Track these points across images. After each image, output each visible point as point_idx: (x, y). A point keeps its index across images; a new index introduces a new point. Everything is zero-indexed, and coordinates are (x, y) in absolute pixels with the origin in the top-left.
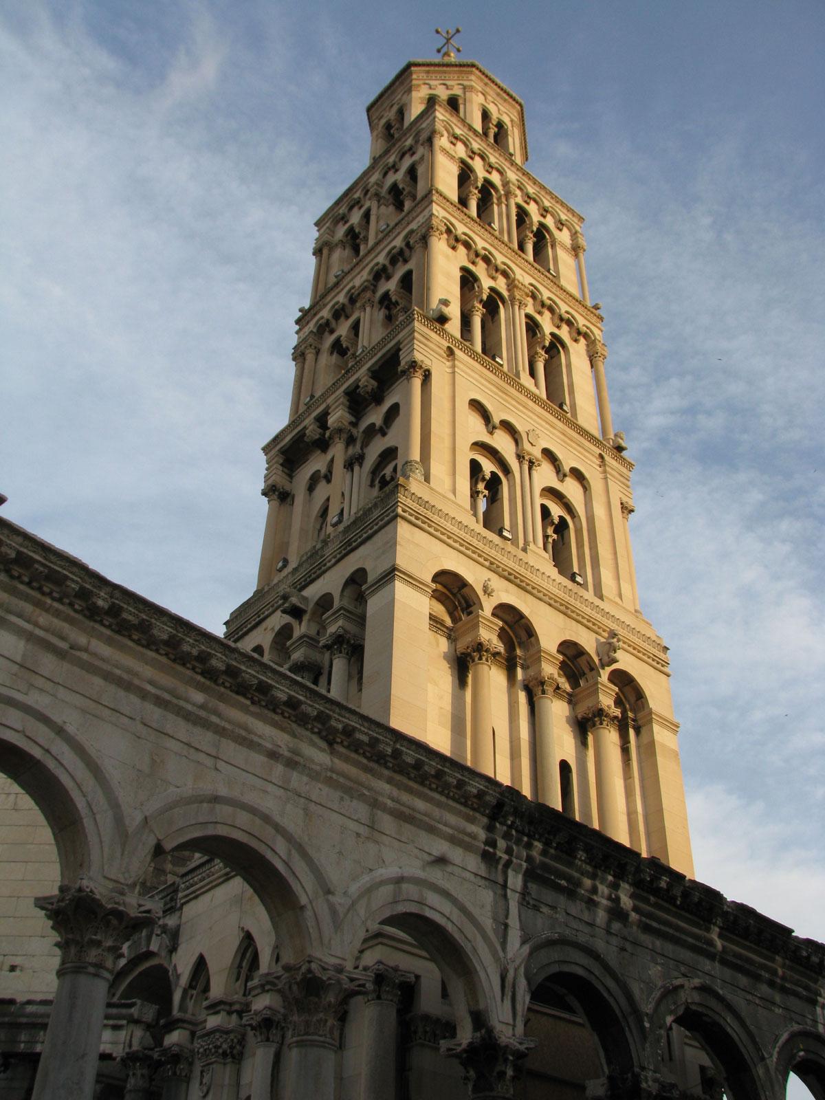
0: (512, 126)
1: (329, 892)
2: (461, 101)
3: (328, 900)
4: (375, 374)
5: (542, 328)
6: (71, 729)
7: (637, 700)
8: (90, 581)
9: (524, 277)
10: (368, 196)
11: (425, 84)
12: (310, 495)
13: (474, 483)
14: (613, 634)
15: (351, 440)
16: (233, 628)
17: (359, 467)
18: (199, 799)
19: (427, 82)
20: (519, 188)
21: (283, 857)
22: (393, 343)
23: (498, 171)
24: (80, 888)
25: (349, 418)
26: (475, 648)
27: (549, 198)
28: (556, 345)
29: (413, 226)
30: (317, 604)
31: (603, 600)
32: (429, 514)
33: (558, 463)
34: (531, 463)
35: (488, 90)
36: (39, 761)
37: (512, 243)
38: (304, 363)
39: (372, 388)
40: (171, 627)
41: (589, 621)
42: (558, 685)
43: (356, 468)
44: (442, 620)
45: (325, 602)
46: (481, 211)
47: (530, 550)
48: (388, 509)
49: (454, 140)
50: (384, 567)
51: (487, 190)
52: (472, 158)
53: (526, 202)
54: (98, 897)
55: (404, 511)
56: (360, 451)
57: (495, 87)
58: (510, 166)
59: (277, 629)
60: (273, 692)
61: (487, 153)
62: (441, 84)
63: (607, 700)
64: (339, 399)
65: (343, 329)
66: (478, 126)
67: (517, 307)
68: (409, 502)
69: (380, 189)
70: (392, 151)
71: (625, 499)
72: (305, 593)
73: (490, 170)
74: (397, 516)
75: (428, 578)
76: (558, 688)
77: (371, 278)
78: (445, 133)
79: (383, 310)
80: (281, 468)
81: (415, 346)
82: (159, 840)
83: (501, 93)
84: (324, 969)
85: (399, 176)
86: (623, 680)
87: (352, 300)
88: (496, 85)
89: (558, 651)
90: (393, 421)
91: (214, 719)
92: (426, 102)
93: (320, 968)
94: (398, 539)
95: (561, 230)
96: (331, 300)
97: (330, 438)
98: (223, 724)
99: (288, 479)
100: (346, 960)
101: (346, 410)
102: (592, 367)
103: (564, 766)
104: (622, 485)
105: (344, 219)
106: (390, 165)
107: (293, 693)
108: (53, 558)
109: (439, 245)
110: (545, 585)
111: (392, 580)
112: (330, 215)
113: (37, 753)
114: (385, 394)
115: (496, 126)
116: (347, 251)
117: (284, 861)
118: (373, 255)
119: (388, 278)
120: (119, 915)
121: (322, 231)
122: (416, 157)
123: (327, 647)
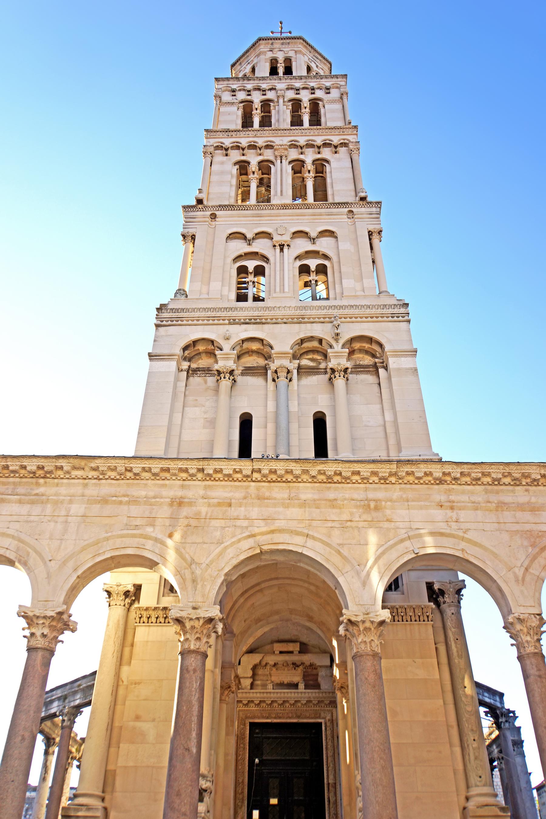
33: (309, 234)
34: (282, 247)
44: (208, 368)
49: (233, 94)
53: (297, 94)
57: (279, 41)
58: (279, 81)
71: (371, 228)
73: (264, 93)
95: (329, 93)
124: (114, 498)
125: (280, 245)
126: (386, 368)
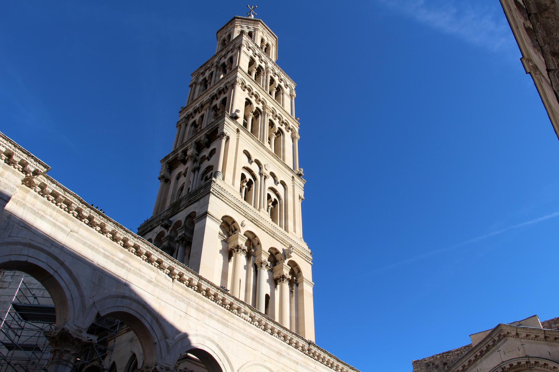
0: (272, 46)
1: (166, 337)
2: (253, 34)
3: (166, 341)
4: (207, 136)
5: (275, 126)
6: (67, 264)
7: (298, 273)
8: (82, 205)
9: (270, 104)
10: (213, 66)
11: (240, 26)
12: (177, 181)
13: (242, 182)
14: (291, 246)
15: (195, 161)
17: (197, 172)
18: (117, 297)
19: (241, 25)
20: (272, 70)
21: (150, 323)
22: (216, 124)
23: (265, 62)
24: (63, 328)
25: (196, 152)
26: (236, 247)
27: (283, 75)
28: (280, 132)
29: (229, 80)
30: (175, 224)
31: (288, 233)
32: (223, 193)
35: (264, 31)
36: (52, 275)
37: (267, 91)
38: (180, 129)
39: (206, 142)
40: (114, 227)
41: (282, 241)
42: (267, 264)
43: (196, 172)
45: (178, 223)
46: (257, 77)
47: (262, 211)
48: (206, 190)
50: (202, 212)
51: (260, 69)
52: (255, 57)
53: (274, 76)
54: (70, 332)
55: (213, 191)
56: (199, 166)
59: (158, 232)
60: (152, 256)
61: (262, 55)
62: (246, 27)
63: (286, 271)
64: (192, 145)
65: (197, 117)
66: (259, 44)
67: (266, 116)
68: (215, 187)
69: (218, 64)
70: (224, 50)
72: (170, 219)
73: (262, 62)
74: (210, 192)
75: (220, 218)
76: (267, 265)
77: (210, 98)
78: (246, 46)
79: (214, 111)
80: (167, 169)
81: (224, 127)
82: (99, 311)
83: (269, 33)
84: (162, 368)
85: (225, 60)
86: (293, 264)
87: (202, 106)
88: (268, 29)
89: (269, 251)
90: (213, 155)
91: (127, 265)
92: (240, 32)
93: (160, 368)
94: (210, 201)
95: (287, 88)
96: (194, 105)
97: (187, 159)
98: (130, 267)
99: (169, 173)
100: (170, 365)
101: (195, 149)
102: (293, 142)
103: (267, 297)
104: (300, 189)
105: (203, 74)
106: (223, 55)
107: (160, 257)
108: (68, 194)
109: (238, 88)
110: (266, 224)
111: (206, 217)
113: (51, 272)
115: (266, 45)
116: (202, 86)
117: (149, 324)
118: (212, 90)
119: (217, 99)
120: (79, 341)
122: (233, 54)
123: (177, 241)
124: (257, 339)
125: (265, 176)
126: (297, 285)
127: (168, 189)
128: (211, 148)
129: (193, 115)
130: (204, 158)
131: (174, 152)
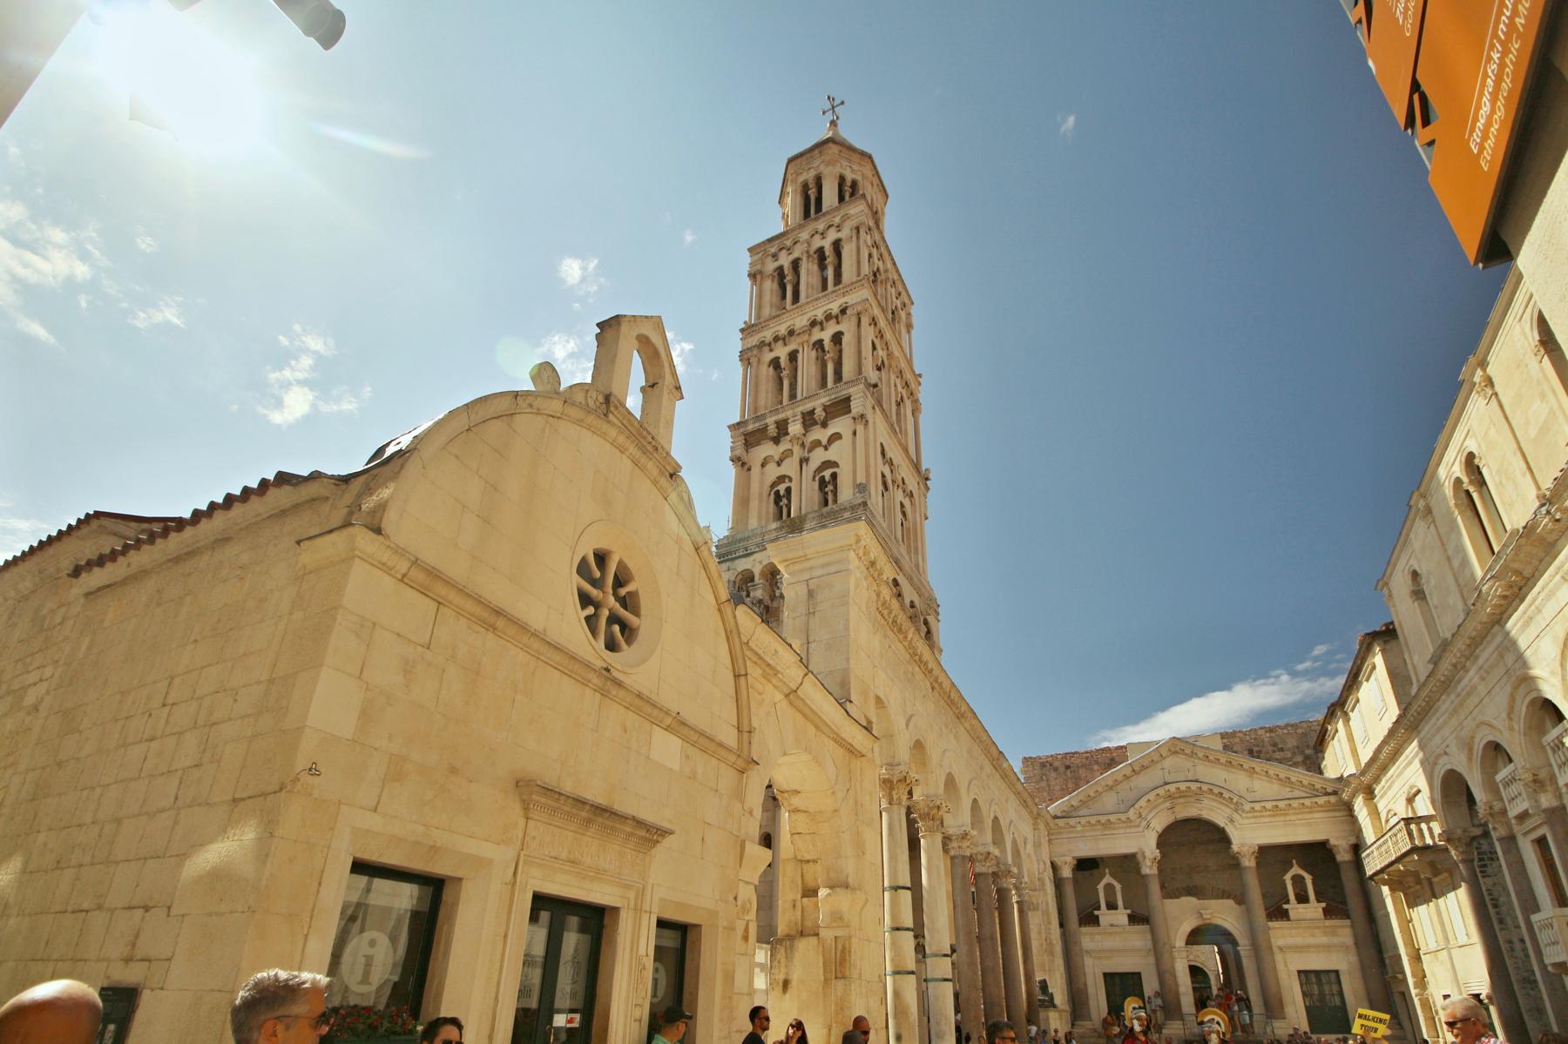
4: (825, 408)
15: (803, 445)
16: (723, 551)
34: (898, 486)
43: (804, 465)
52: (873, 247)
79: (815, 350)
87: (791, 333)
105: (775, 256)
112: (762, 249)
114: (829, 422)
119: (822, 329)
121: (756, 257)
127: (749, 479)
128: (831, 430)
129: (773, 343)
130: (817, 443)
131: (757, 419)
